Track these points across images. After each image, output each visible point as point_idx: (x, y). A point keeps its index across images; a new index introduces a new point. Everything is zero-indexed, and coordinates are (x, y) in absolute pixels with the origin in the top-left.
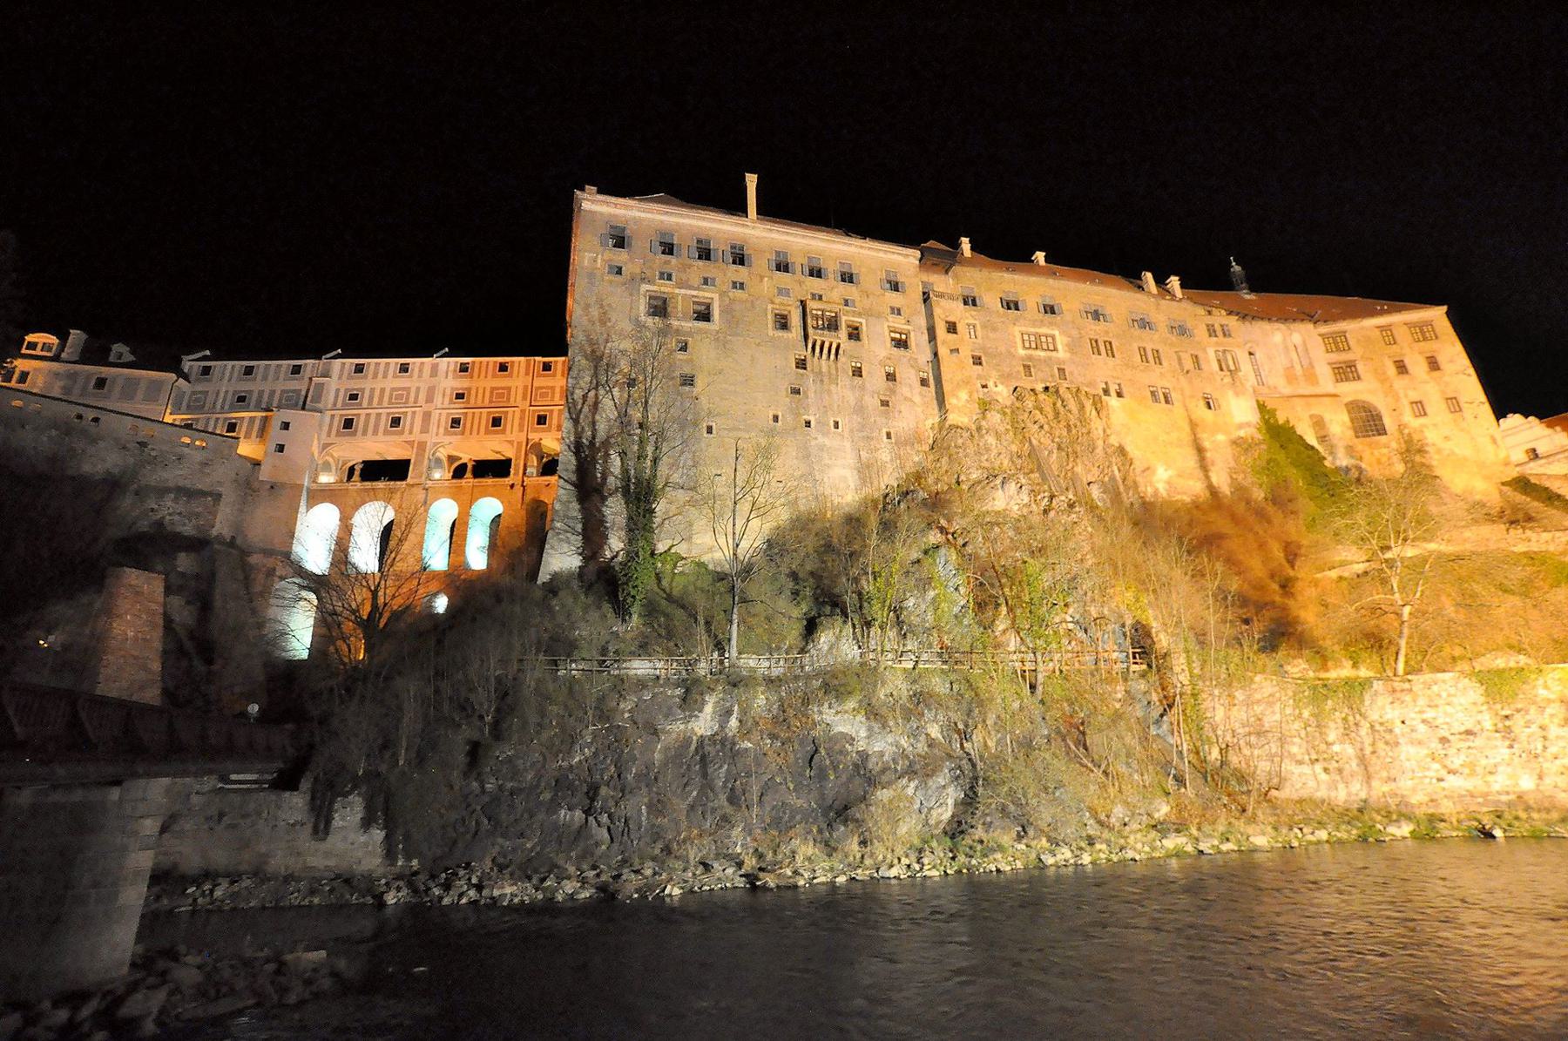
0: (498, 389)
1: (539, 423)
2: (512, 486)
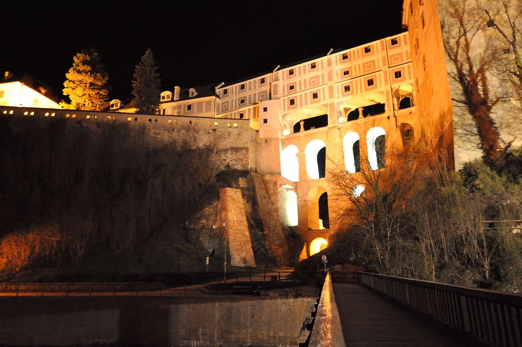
0: (367, 63)
1: (396, 77)
2: (388, 117)
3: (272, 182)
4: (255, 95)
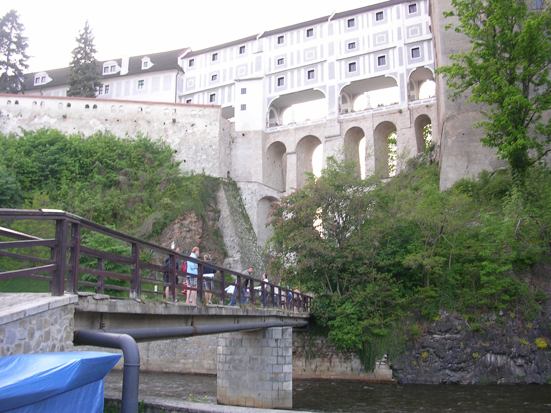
3: (250, 192)
4: (231, 69)
